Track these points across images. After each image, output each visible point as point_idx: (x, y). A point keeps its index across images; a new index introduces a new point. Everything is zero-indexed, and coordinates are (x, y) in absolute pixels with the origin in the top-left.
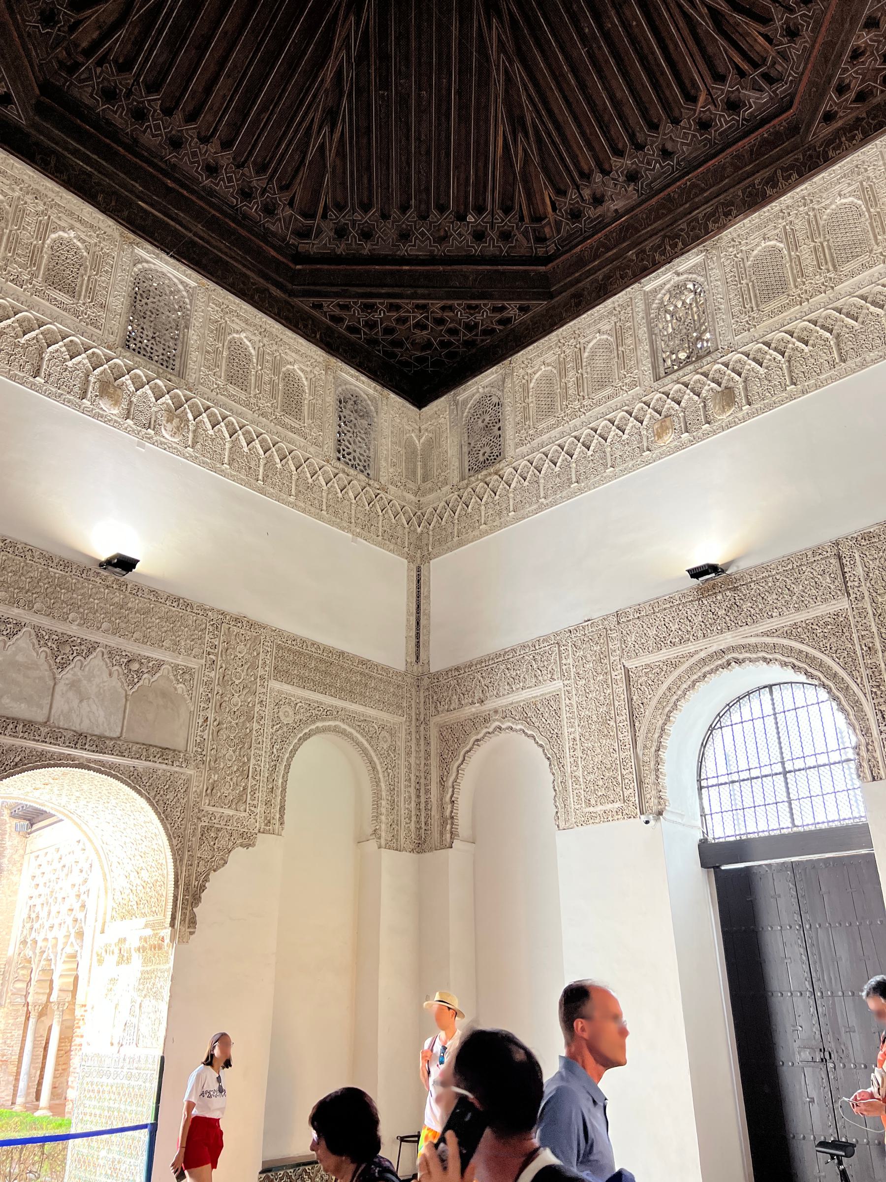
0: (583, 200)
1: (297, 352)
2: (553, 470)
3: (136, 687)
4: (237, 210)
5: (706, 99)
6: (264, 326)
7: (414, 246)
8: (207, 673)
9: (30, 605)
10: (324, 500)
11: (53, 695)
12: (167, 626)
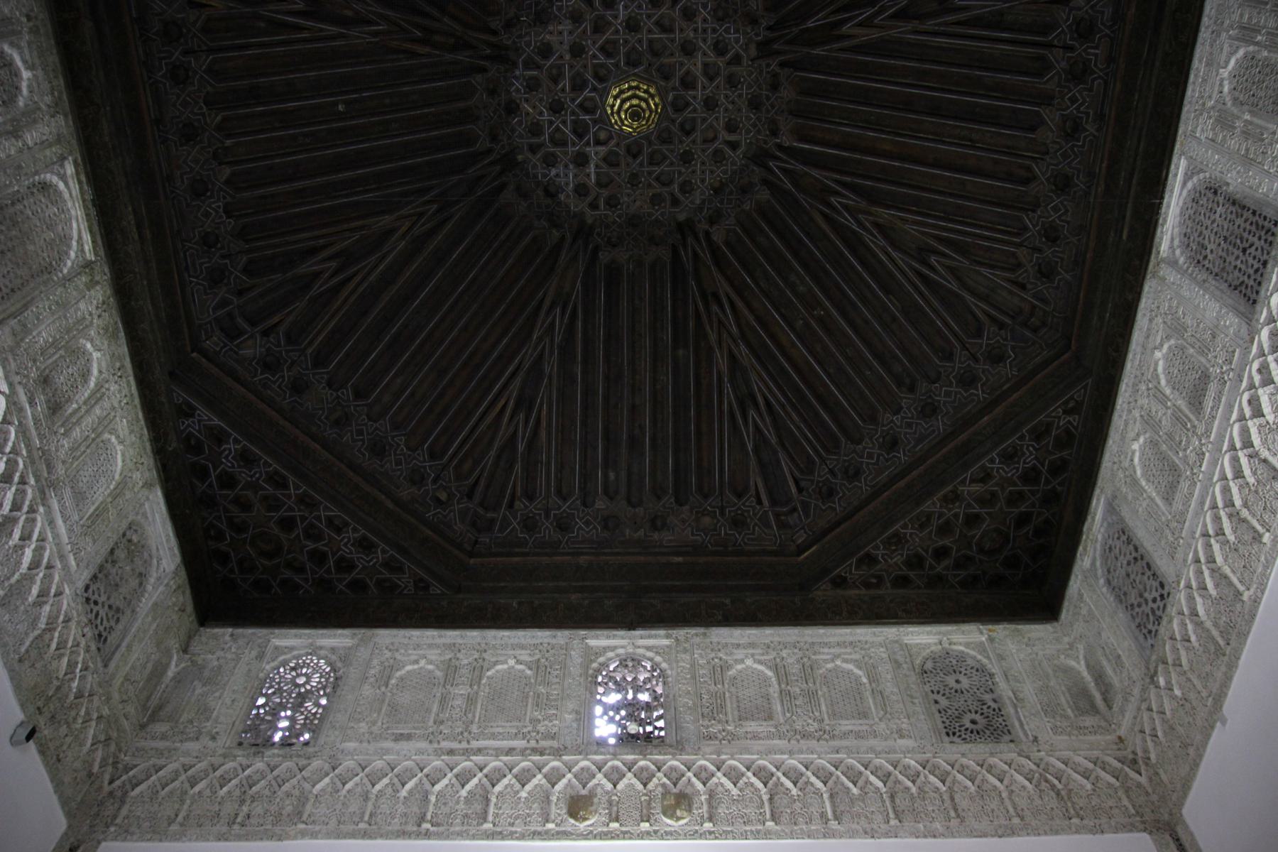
4: (1107, 74)
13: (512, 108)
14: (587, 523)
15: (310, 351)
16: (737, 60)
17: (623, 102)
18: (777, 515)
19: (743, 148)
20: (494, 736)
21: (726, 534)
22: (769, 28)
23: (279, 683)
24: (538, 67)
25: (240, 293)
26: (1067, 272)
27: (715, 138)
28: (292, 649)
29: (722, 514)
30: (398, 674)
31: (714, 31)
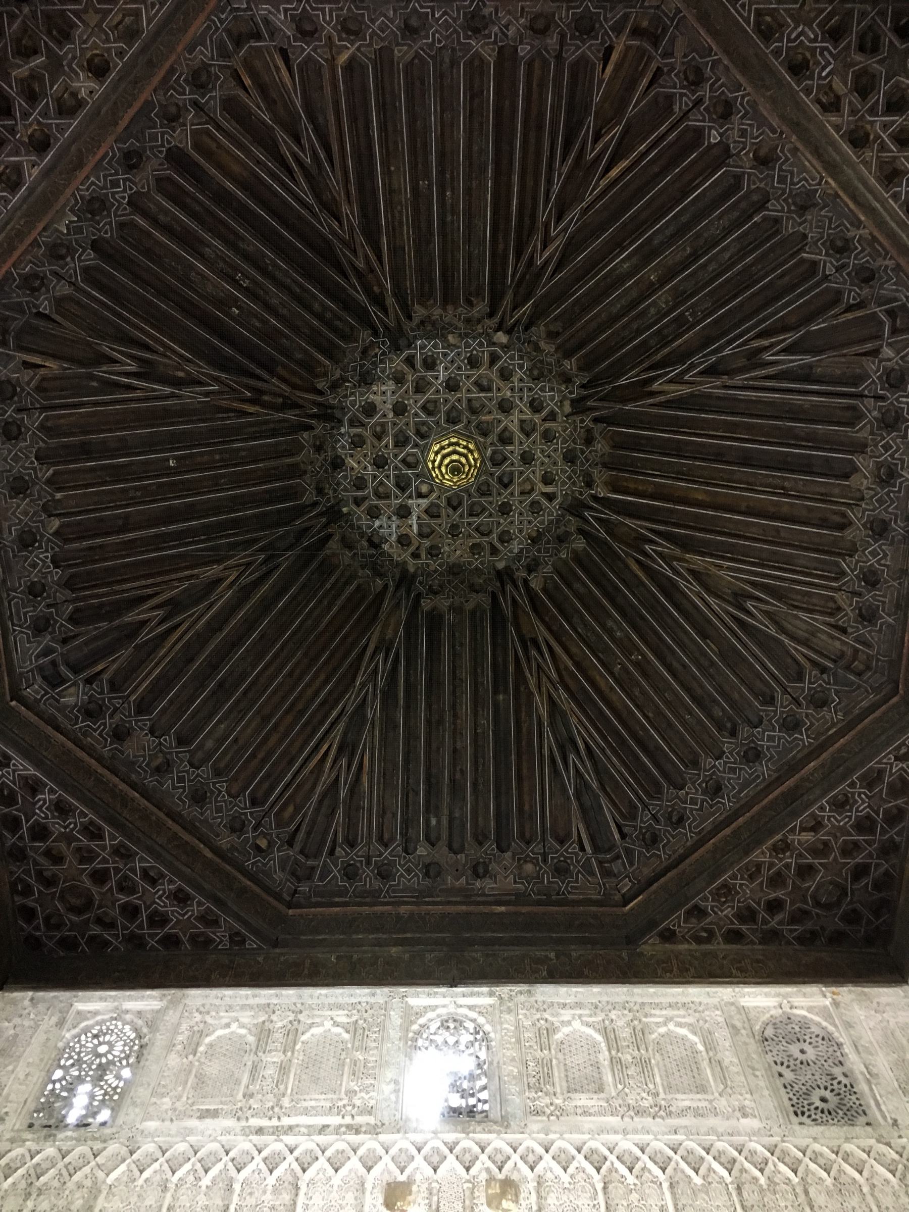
0: (563, 36)
5: (339, 53)
13: (337, 464)
14: (409, 871)
15: (133, 698)
16: (552, 416)
17: (444, 457)
18: (600, 863)
19: (559, 500)
20: (306, 1112)
21: (549, 882)
22: (583, 386)
23: (79, 1053)
24: (363, 425)
25: (65, 641)
26: (889, 615)
27: (532, 490)
28: (96, 1013)
29: (545, 861)
30: (208, 1040)
31: (530, 389)
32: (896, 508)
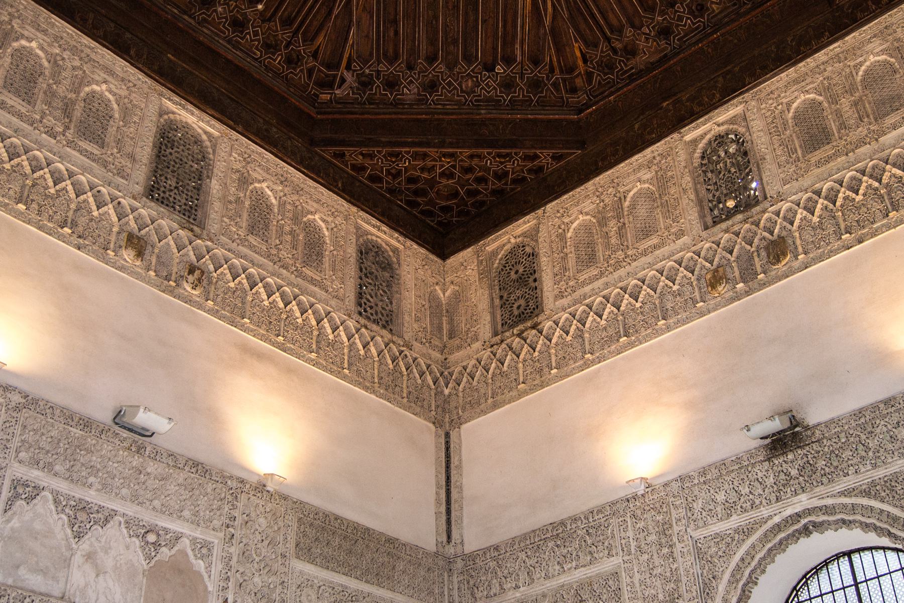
1: (318, 201)
2: (598, 323)
3: (153, 562)
6: (285, 175)
7: (441, 95)
8: (226, 549)
9: (48, 467)
10: (346, 358)
11: (69, 566)
12: (186, 494)
32: (214, 19)
